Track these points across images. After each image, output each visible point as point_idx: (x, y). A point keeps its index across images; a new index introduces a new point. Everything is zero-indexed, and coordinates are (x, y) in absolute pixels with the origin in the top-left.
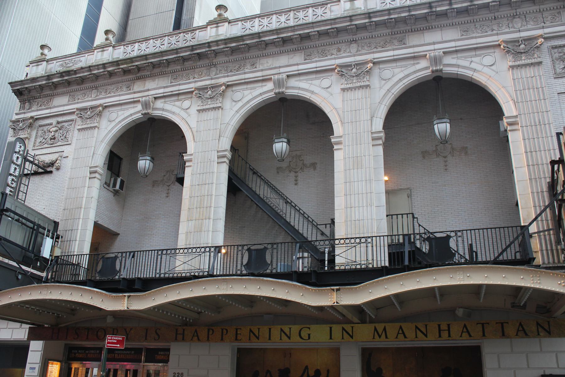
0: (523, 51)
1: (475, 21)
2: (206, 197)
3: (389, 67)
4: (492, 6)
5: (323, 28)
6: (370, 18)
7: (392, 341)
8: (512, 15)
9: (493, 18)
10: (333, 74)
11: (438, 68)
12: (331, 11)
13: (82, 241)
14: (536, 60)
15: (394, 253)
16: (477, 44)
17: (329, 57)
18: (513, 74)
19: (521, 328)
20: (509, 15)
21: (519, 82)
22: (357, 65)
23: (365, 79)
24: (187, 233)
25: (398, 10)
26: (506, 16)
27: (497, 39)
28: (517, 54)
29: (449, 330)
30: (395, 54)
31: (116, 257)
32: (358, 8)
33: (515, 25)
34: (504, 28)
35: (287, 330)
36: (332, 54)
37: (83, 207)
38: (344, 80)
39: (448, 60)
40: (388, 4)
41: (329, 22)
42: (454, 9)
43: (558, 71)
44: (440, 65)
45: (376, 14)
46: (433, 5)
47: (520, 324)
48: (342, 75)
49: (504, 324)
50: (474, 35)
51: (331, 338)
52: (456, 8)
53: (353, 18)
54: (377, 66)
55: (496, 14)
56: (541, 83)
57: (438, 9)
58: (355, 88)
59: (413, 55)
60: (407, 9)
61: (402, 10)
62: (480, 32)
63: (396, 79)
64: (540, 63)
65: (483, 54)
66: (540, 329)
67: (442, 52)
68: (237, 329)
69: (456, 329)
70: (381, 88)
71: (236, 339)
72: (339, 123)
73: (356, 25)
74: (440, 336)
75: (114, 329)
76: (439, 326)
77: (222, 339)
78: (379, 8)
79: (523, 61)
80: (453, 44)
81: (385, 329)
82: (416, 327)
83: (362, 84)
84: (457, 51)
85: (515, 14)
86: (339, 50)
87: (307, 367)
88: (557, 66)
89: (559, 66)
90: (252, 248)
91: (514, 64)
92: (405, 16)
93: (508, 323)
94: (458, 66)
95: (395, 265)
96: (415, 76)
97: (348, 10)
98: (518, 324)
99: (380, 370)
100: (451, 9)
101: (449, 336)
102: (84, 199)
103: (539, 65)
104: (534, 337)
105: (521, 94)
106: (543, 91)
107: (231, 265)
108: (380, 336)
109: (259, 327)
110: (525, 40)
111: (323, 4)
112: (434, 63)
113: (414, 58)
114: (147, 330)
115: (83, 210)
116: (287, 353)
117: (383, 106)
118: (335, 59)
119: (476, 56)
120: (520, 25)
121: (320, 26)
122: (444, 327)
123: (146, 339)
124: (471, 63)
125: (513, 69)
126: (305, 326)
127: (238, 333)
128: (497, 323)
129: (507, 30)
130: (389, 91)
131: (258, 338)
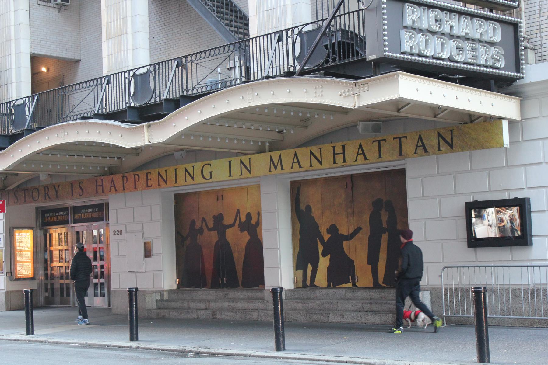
2: (121, 3)
7: (329, 169)
13: (19, 82)
15: (343, 43)
19: (420, 144)
24: (108, 55)
29: (344, 153)
31: (25, 103)
35: (190, 170)
37: (13, 37)
47: (420, 138)
49: (402, 139)
51: (230, 175)
66: (442, 142)
68: (147, 174)
69: (351, 151)
71: (148, 186)
74: (335, 162)
75: (45, 187)
76: (334, 147)
77: (135, 188)
81: (280, 158)
82: (311, 153)
87: (238, 211)
90: (137, 73)
93: (406, 137)
95: (344, 58)
98: (417, 138)
99: (309, 208)
101: (344, 161)
102: (12, 28)
104: (434, 154)
107: (177, 86)
108: (276, 168)
109: (166, 168)
114: (72, 184)
115: (13, 43)
116: (219, 195)
122: (339, 150)
123: (72, 196)
126: (206, 162)
127: (149, 178)
128: (394, 138)
131: (166, 182)
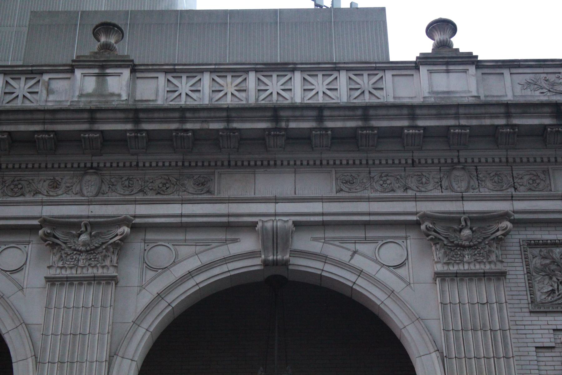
0: (467, 243)
1: (370, 162)
3: (169, 241)
4: (408, 135)
5: (22, 128)
6: (137, 121)
8: (449, 161)
9: (410, 161)
10: (34, 239)
11: (279, 257)
12: (49, 92)
14: (493, 266)
16: (369, 214)
17: (28, 198)
18: (442, 292)
20: (443, 161)
21: (454, 313)
22: (93, 225)
23: (107, 263)
25: (203, 114)
26: (436, 161)
27: (414, 210)
28: (454, 249)
30: (185, 212)
32: (112, 95)
33: (454, 184)
34: (430, 187)
36: (37, 193)
38: (56, 258)
39: (304, 242)
40: (183, 96)
41: (40, 116)
42: (327, 129)
43: (540, 297)
44: (285, 249)
45: (151, 115)
46: (282, 113)
48: (54, 245)
50: (366, 194)
52: (332, 129)
53: (98, 115)
54: (141, 236)
55: (417, 154)
56: (501, 319)
57: (292, 125)
58: (81, 281)
59: (225, 219)
60: (224, 114)
61: (212, 114)
62: (379, 188)
63: (180, 271)
64: (501, 275)
65: (382, 238)
67: (290, 223)
70: (142, 287)
72: (31, 362)
73: (102, 132)
78: (160, 102)
79: (466, 267)
80: (317, 207)
83: (100, 272)
84: (324, 225)
85: (456, 160)
86: (55, 185)
88: (537, 286)
89: (541, 285)
91: (445, 269)
92: (218, 130)
94: (325, 259)
96: (224, 268)
97: (88, 95)
100: (321, 129)
103: (499, 279)
105: (457, 339)
106: (504, 338)
110: (472, 220)
111: (32, 72)
112: (270, 244)
113: (228, 227)
117: (141, 331)
118: (42, 203)
119: (366, 240)
120: (464, 185)
121: (17, 122)
124: (352, 256)
125: (443, 280)
129: (437, 193)
130: (160, 296)
